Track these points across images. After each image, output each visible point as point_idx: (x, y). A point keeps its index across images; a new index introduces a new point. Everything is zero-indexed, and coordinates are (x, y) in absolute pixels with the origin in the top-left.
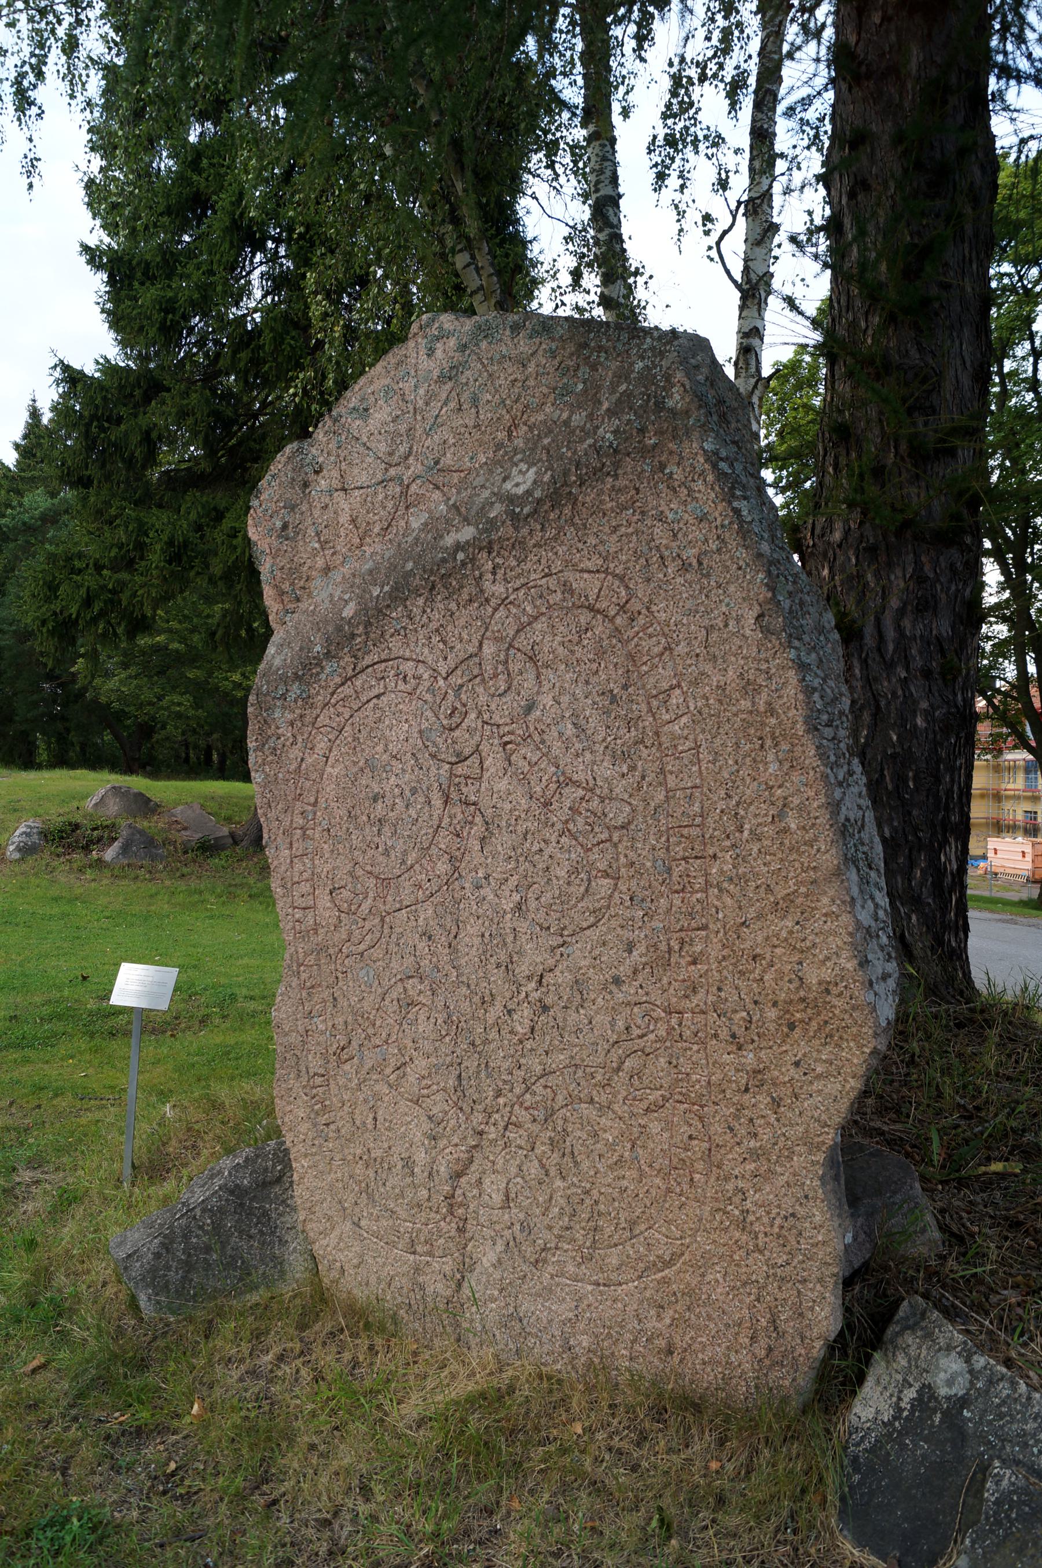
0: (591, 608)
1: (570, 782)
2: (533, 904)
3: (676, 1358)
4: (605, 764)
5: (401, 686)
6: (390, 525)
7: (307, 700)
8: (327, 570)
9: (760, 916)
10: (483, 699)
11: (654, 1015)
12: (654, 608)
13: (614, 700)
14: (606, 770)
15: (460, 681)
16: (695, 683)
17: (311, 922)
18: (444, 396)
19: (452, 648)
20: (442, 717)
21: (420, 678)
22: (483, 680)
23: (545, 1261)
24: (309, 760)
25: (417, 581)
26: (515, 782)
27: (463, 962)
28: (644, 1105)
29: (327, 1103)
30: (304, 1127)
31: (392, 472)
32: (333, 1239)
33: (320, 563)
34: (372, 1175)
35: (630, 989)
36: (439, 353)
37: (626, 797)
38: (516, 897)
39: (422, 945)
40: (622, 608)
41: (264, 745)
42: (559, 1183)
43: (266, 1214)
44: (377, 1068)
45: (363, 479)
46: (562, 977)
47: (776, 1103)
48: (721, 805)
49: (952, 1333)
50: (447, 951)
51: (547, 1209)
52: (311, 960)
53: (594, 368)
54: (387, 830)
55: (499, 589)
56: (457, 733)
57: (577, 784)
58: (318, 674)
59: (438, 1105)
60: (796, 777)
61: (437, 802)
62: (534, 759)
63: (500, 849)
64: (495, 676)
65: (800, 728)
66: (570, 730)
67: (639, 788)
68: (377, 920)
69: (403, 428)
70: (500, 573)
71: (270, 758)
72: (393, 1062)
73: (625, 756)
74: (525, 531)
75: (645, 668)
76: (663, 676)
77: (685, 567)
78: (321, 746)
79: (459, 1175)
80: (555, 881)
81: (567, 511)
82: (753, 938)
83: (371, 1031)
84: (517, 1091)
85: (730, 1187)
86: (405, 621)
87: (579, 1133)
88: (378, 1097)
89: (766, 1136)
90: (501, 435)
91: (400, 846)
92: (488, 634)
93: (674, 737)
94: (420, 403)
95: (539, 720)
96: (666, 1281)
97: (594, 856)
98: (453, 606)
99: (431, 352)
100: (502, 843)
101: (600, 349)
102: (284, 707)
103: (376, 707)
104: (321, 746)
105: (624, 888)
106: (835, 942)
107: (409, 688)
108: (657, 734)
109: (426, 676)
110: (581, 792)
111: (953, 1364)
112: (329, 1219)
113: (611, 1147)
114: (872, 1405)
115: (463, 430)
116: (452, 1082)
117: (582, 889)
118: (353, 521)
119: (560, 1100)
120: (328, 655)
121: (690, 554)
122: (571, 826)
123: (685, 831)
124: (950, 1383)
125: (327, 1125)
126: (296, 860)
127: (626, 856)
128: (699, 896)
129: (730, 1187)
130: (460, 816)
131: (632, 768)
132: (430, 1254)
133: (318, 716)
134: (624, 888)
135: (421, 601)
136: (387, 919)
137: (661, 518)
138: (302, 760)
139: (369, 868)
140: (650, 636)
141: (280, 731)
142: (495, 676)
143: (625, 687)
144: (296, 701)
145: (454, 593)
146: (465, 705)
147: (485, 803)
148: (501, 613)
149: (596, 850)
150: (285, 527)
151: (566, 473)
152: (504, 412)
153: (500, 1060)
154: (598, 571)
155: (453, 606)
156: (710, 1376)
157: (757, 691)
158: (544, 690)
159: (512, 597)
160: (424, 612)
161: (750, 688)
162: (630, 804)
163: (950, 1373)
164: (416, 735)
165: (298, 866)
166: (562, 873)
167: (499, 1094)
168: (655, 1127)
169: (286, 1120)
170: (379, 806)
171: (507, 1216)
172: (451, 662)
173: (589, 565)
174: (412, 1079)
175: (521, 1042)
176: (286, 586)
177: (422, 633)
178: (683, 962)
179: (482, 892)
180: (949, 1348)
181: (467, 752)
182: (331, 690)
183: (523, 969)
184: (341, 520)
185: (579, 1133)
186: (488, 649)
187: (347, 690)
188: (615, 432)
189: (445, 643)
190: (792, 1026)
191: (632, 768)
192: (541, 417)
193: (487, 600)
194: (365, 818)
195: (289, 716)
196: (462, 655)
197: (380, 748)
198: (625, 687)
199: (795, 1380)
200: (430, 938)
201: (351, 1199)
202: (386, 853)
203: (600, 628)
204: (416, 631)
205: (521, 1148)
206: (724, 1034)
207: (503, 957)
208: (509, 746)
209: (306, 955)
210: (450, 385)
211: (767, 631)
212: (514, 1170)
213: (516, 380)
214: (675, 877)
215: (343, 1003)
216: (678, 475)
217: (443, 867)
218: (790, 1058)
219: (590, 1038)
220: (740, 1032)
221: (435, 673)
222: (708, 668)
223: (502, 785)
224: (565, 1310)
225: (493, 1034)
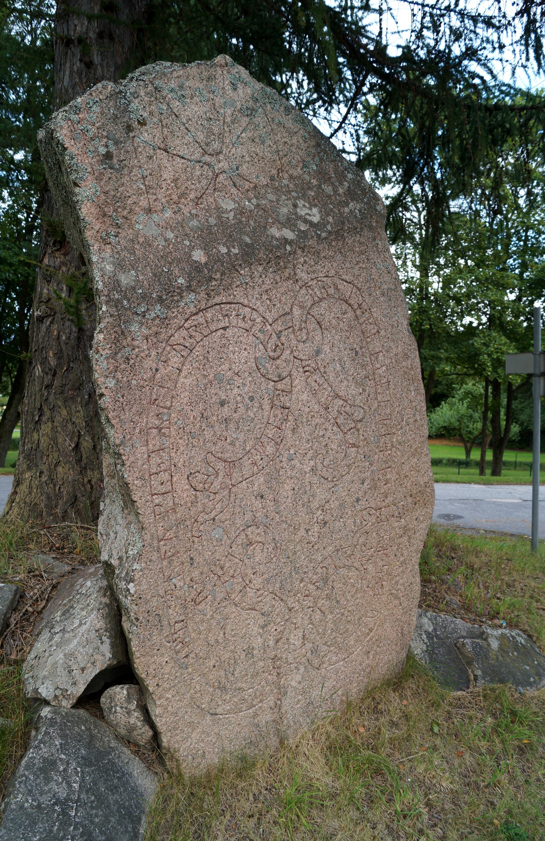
1: (337, 396)
2: (320, 467)
4: (353, 387)
6: (201, 197)
7: (164, 321)
8: (149, 211)
10: (294, 342)
11: (371, 513)
12: (372, 310)
14: (354, 390)
15: (280, 329)
17: (171, 504)
18: (244, 125)
19: (274, 305)
20: (269, 350)
21: (254, 320)
22: (294, 330)
23: (323, 663)
24: (162, 371)
26: (311, 396)
27: (282, 508)
28: (367, 557)
29: (187, 640)
31: (207, 158)
33: (144, 203)
34: (222, 673)
37: (362, 405)
38: (312, 463)
39: (258, 504)
41: (116, 354)
42: (330, 616)
46: (334, 504)
50: (273, 503)
51: (324, 634)
54: (232, 426)
56: (278, 362)
58: (178, 301)
62: (321, 383)
63: (304, 435)
64: (301, 329)
66: (338, 368)
67: (368, 400)
68: (226, 492)
71: (123, 366)
72: (238, 588)
75: (369, 339)
78: (175, 360)
80: (330, 451)
81: (340, 244)
86: (248, 279)
87: (339, 585)
90: (274, 172)
91: (241, 436)
92: (296, 302)
93: (380, 376)
94: (228, 119)
95: (323, 360)
98: (278, 278)
100: (305, 431)
102: (142, 324)
103: (223, 336)
105: (362, 452)
107: (247, 326)
108: (374, 373)
109: (258, 320)
110: (341, 402)
115: (254, 155)
117: (343, 454)
118: (175, 180)
119: (331, 571)
120: (189, 288)
122: (338, 421)
123: (385, 422)
125: (187, 656)
126: (153, 455)
127: (363, 435)
128: (389, 452)
130: (280, 416)
131: (364, 390)
133: (173, 335)
134: (362, 452)
135: (260, 269)
136: (233, 490)
138: (157, 370)
139: (220, 455)
140: (370, 324)
141: (136, 343)
142: (301, 329)
143: (361, 348)
144: (153, 320)
145: (279, 270)
146: (283, 344)
148: (303, 291)
149: (349, 433)
150: (108, 156)
152: (278, 158)
154: (350, 283)
155: (278, 278)
158: (325, 343)
159: (310, 283)
160: (261, 276)
162: (363, 408)
164: (252, 360)
169: (151, 670)
170: (226, 408)
171: (304, 650)
173: (347, 278)
175: (313, 547)
176: (110, 210)
178: (382, 484)
179: (293, 462)
182: (187, 316)
183: (315, 504)
184: (165, 176)
185: (339, 585)
186: (297, 312)
187: (199, 318)
189: (270, 300)
191: (364, 390)
193: (297, 280)
194: (215, 418)
196: (281, 312)
200: (262, 497)
201: (207, 699)
202: (232, 444)
204: (254, 288)
205: (309, 607)
206: (396, 514)
208: (307, 373)
213: (286, 143)
215: (198, 559)
217: (270, 449)
222: (392, 344)
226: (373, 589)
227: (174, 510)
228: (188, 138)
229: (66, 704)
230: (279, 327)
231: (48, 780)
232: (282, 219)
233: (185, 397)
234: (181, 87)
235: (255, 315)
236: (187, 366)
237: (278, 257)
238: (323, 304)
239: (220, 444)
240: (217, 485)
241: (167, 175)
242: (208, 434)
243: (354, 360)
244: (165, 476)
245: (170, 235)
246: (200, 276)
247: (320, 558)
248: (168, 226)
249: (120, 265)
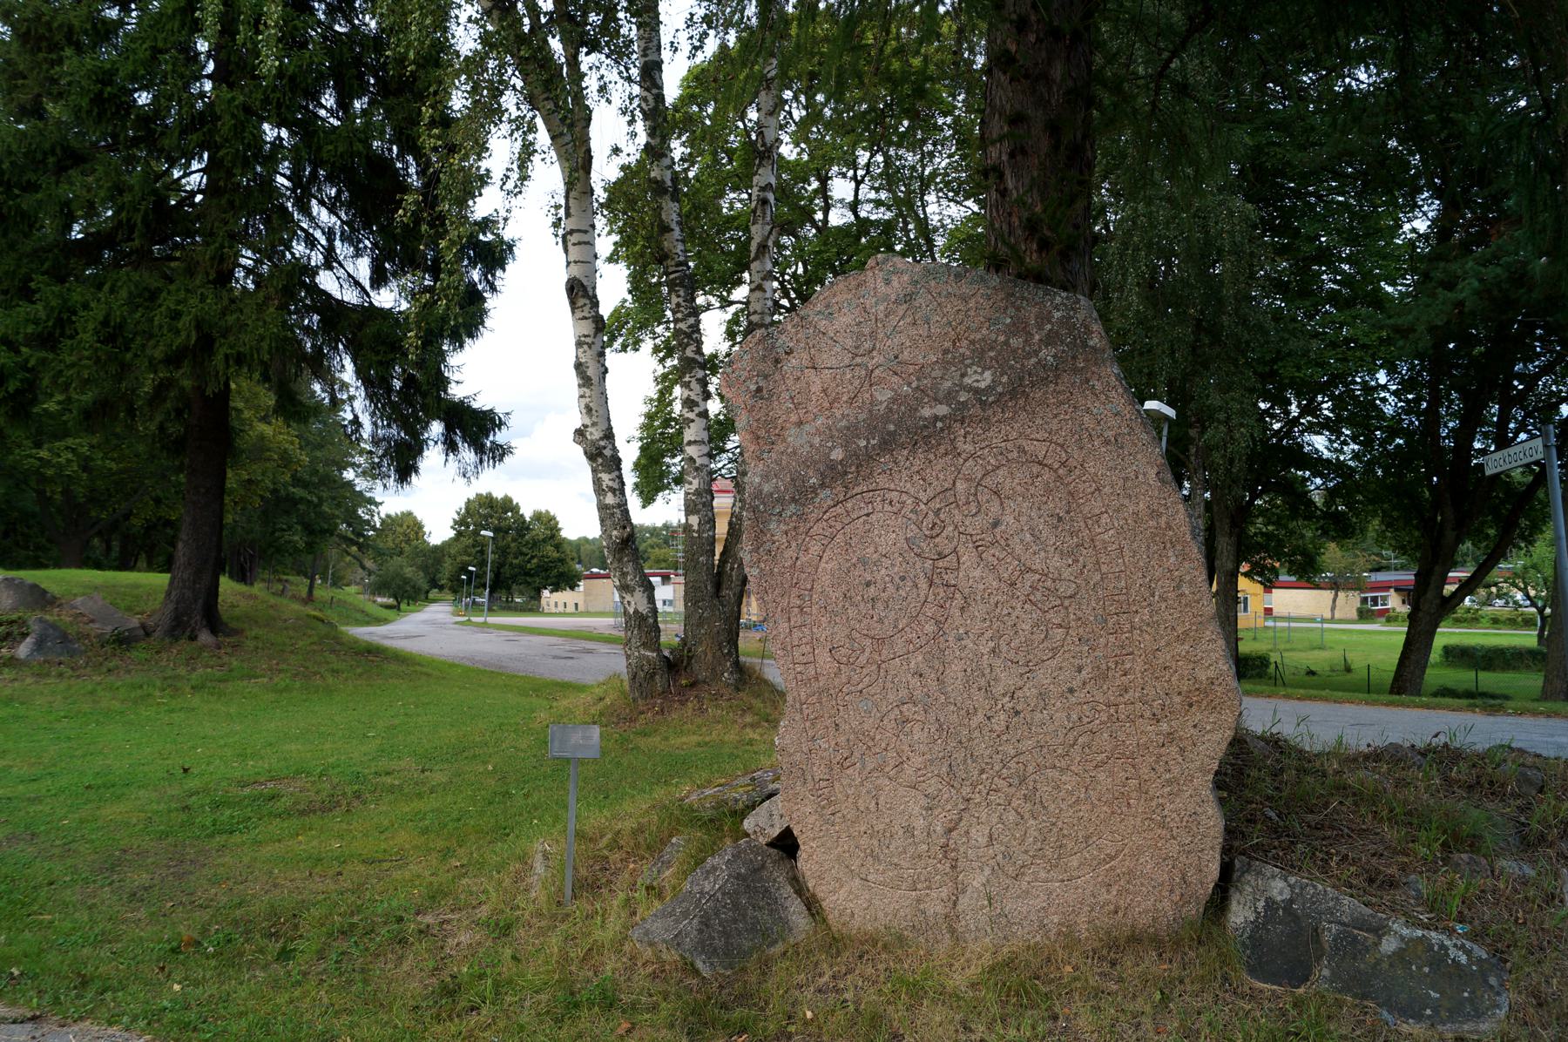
0: (1040, 463)
2: (1004, 648)
3: (1120, 914)
5: (887, 508)
7: (802, 517)
8: (800, 423)
9: (1168, 644)
10: (958, 518)
13: (1060, 519)
14: (1056, 562)
16: (1118, 511)
25: (903, 439)
30: (811, 819)
31: (859, 360)
32: (843, 893)
33: (794, 418)
34: (876, 842)
35: (1081, 695)
36: (895, 284)
39: (915, 682)
40: (1063, 464)
42: (1032, 822)
43: (767, 890)
44: (879, 768)
45: (833, 362)
46: (1030, 692)
47: (1182, 750)
48: (1140, 581)
49: (1269, 870)
52: (814, 699)
53: (1018, 309)
54: (880, 605)
55: (969, 448)
57: (1035, 571)
59: (932, 786)
60: (1186, 565)
61: (923, 584)
65: (1188, 537)
68: (874, 667)
69: (867, 331)
70: (969, 438)
72: (892, 763)
73: (1070, 554)
74: (990, 412)
76: (1096, 506)
77: (1107, 442)
78: (815, 549)
79: (950, 831)
81: (1021, 402)
82: (1164, 657)
83: (871, 744)
84: (997, 768)
85: (1154, 804)
86: (891, 465)
88: (879, 788)
89: (1176, 770)
93: (1104, 542)
94: (881, 316)
96: (1112, 869)
97: (1050, 615)
98: (931, 456)
99: (888, 282)
100: (978, 610)
101: (1023, 298)
104: (815, 549)
106: (1214, 656)
111: (1279, 884)
112: (838, 880)
113: (1071, 793)
114: (1240, 914)
116: (944, 769)
118: (824, 391)
119: (1031, 769)
120: (823, 485)
121: (1109, 434)
124: (1281, 893)
129: (1154, 804)
132: (928, 888)
135: (905, 452)
137: (1088, 411)
143: (1068, 512)
147: (962, 584)
148: (971, 462)
150: (759, 390)
151: (1021, 379)
153: (982, 749)
155: (931, 456)
156: (1144, 920)
157: (1160, 515)
161: (1155, 514)
163: (1279, 889)
165: (797, 634)
166: (1027, 627)
167: (982, 771)
168: (1101, 776)
170: (872, 588)
172: (930, 492)
174: (910, 771)
176: (762, 433)
177: (905, 473)
180: (1273, 877)
181: (946, 552)
183: (999, 689)
186: (961, 486)
187: (839, 509)
188: (1054, 356)
190: (1191, 705)
192: (979, 336)
195: (784, 528)
196: (939, 489)
197: (871, 550)
198: (1068, 512)
199: (1193, 910)
201: (858, 862)
202: (881, 621)
203: (1047, 475)
206: (1148, 714)
207: (983, 682)
209: (808, 696)
210: (905, 306)
211: (1162, 481)
212: (995, 820)
214: (1110, 625)
215: (843, 726)
216: (1098, 386)
217: (930, 628)
218: (1190, 723)
219: (1051, 728)
220: (1158, 712)
221: (917, 500)
222: (1126, 502)
223: (977, 573)
224: (1040, 903)
225: (976, 734)
226: (1109, 803)
227: (817, 679)
228: (838, 349)
229: (763, 840)
230: (936, 504)
231: (707, 878)
232: (941, 395)
233: (826, 580)
234: (827, 306)
235: (904, 497)
236: (828, 552)
237: (926, 436)
238: (1001, 472)
239: (865, 622)
240: (863, 659)
241: (816, 388)
242: (851, 612)
243: (1056, 528)
244: (808, 648)
245: (817, 440)
246: (833, 474)
247: (1013, 752)
248: (818, 432)
249: (766, 477)
